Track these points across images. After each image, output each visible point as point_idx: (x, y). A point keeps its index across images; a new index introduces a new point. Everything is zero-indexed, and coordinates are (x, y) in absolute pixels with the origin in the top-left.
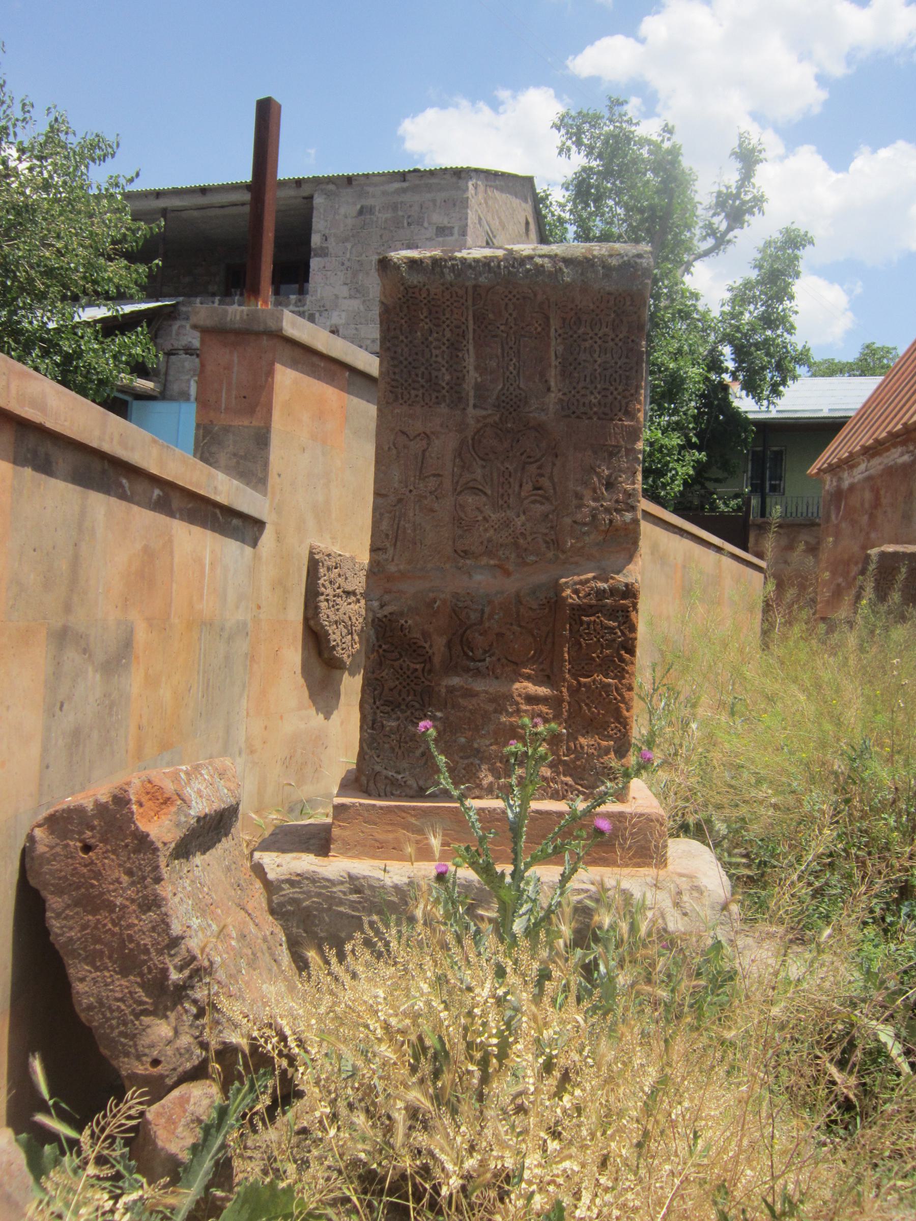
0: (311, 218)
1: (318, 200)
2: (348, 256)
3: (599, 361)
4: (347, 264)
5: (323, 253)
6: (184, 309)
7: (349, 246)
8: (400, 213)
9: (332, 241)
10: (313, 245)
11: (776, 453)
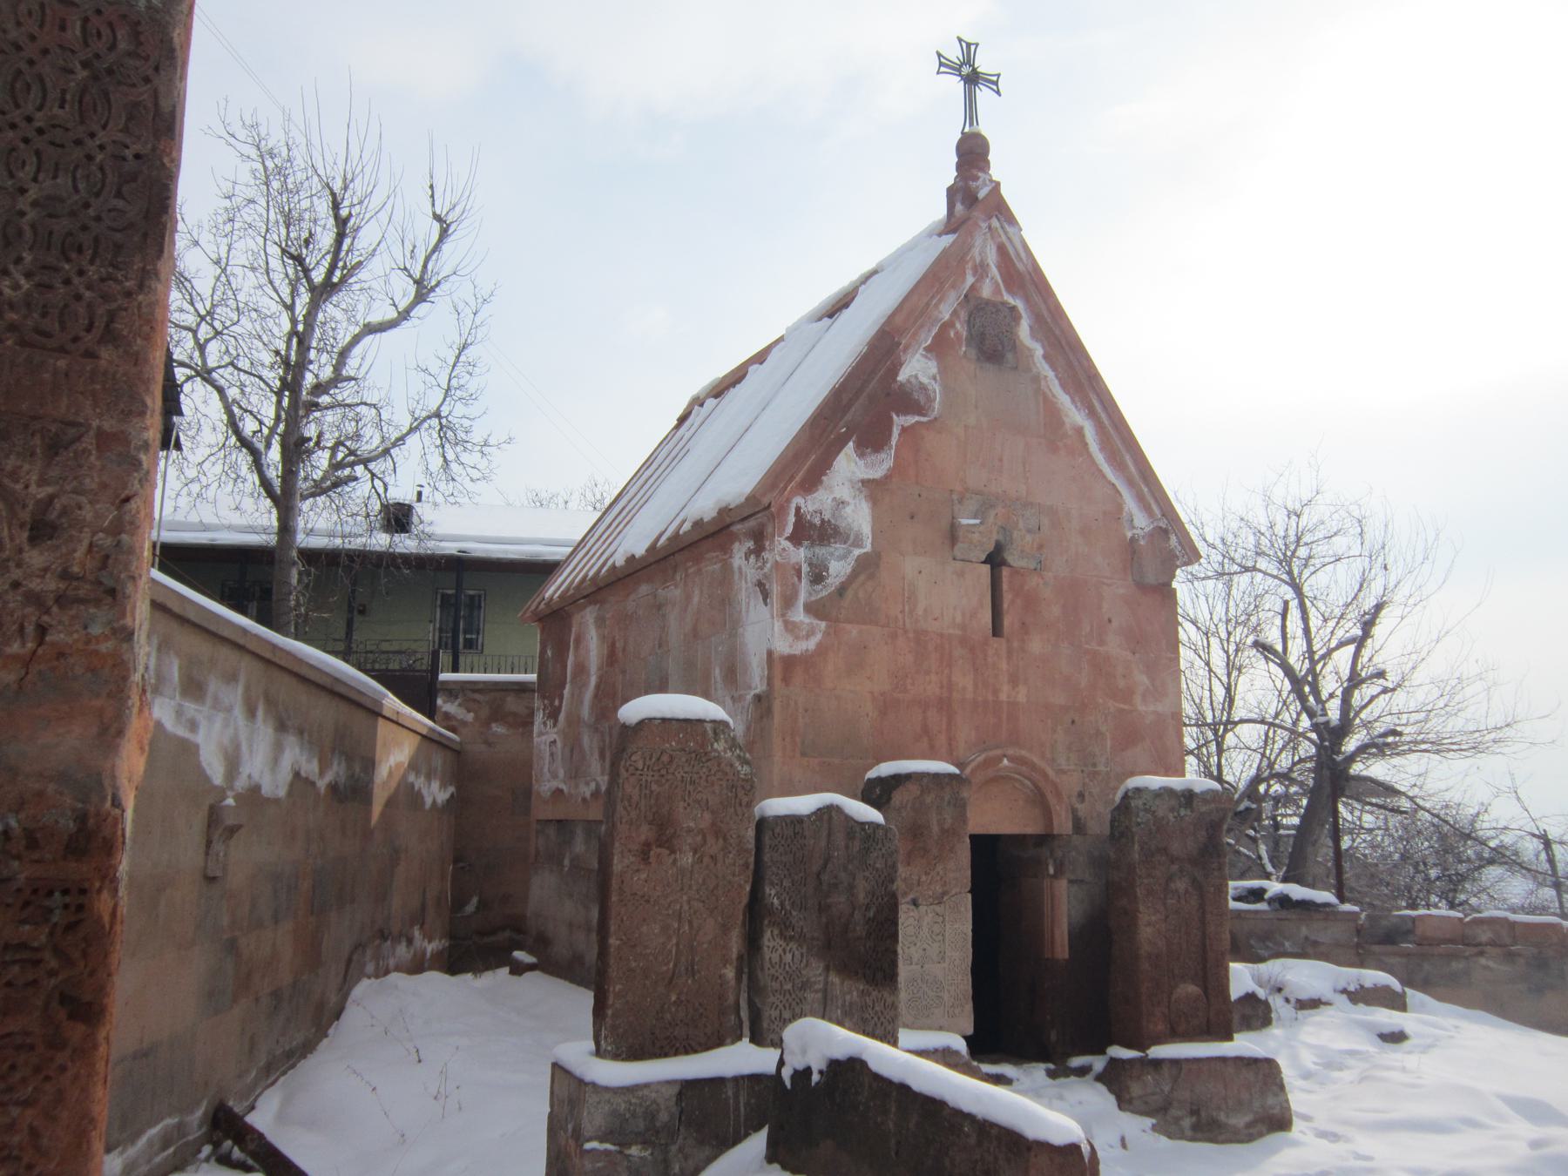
3: (33, 193)
11: (472, 597)
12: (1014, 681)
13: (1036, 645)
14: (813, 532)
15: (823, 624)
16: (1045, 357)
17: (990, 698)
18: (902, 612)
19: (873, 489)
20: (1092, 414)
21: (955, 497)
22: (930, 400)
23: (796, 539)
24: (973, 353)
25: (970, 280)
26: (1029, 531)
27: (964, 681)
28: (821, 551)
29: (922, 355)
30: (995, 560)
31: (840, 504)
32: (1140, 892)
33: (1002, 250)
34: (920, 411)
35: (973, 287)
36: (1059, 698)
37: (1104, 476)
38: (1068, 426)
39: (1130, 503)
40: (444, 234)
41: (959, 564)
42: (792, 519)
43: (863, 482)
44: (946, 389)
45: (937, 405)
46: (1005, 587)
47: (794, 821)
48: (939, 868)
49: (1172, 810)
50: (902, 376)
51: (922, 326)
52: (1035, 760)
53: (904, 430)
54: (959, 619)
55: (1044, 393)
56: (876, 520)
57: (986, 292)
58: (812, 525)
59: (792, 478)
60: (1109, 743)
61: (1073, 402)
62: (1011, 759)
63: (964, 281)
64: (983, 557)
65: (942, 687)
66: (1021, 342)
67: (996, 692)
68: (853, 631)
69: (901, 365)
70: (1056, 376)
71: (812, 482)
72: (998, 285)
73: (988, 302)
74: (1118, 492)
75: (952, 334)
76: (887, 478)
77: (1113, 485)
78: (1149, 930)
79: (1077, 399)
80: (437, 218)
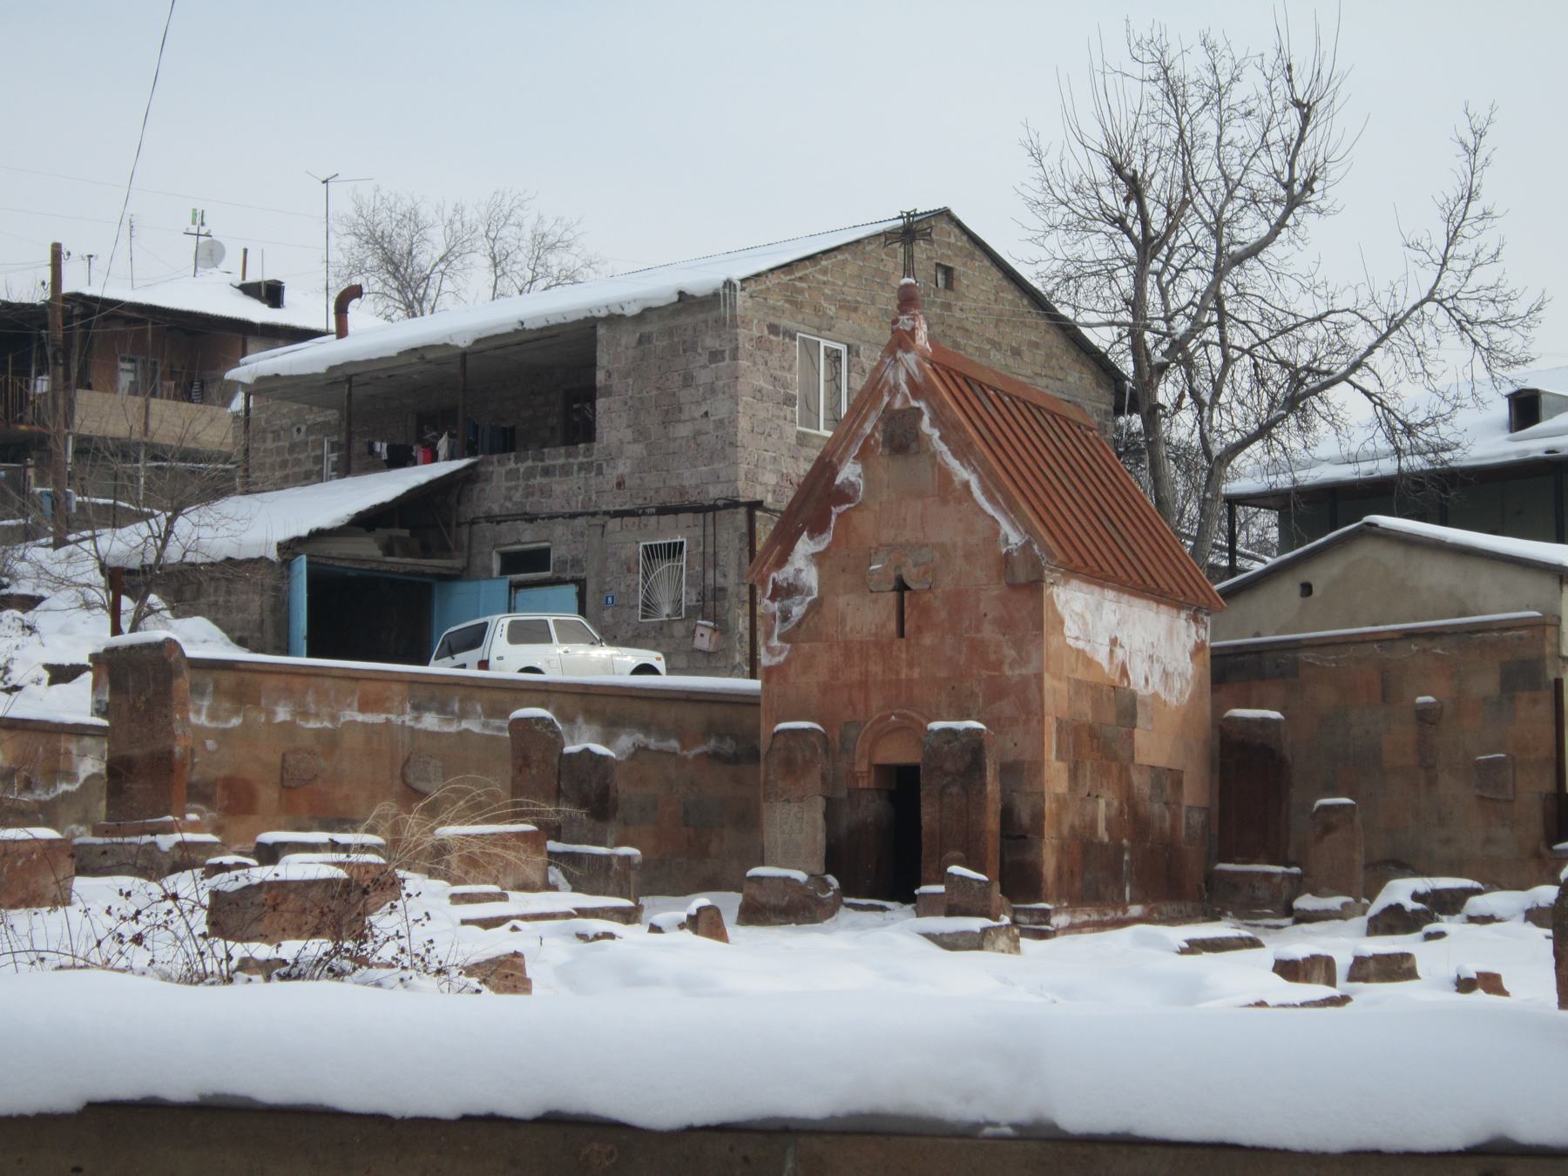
0: (595, 352)
1: (601, 331)
2: (630, 394)
4: (630, 403)
5: (608, 392)
6: (482, 469)
7: (630, 381)
8: (676, 339)
9: (615, 376)
10: (598, 385)
12: (911, 665)
13: (928, 640)
14: (785, 592)
15: (788, 646)
16: (941, 438)
17: (894, 677)
18: (837, 631)
19: (818, 559)
20: (975, 471)
21: (873, 551)
22: (856, 491)
23: (773, 598)
24: (887, 452)
25: (886, 399)
26: (916, 565)
27: (876, 668)
28: (786, 602)
29: (854, 463)
30: (902, 587)
31: (799, 571)
32: (922, 794)
33: (907, 372)
34: (849, 499)
35: (888, 404)
36: (942, 673)
37: (984, 512)
38: (957, 483)
39: (1006, 527)
40: (1306, 119)
41: (874, 595)
42: (770, 586)
43: (814, 555)
44: (867, 481)
45: (861, 494)
46: (906, 604)
47: (570, 755)
48: (802, 782)
49: (948, 742)
50: (838, 481)
51: (851, 442)
52: (914, 715)
53: (839, 516)
54: (873, 631)
55: (940, 466)
56: (820, 577)
57: (898, 404)
58: (782, 587)
59: (764, 564)
60: (981, 700)
61: (962, 464)
62: (897, 716)
63: (882, 400)
64: (891, 587)
65: (861, 674)
66: (923, 433)
67: (898, 673)
68: (806, 647)
69: (837, 473)
70: (949, 449)
71: (782, 561)
72: (906, 395)
73: (899, 411)
74: (997, 522)
75: (872, 442)
76: (828, 549)
78: (927, 817)
79: (964, 461)
80: (1297, 104)
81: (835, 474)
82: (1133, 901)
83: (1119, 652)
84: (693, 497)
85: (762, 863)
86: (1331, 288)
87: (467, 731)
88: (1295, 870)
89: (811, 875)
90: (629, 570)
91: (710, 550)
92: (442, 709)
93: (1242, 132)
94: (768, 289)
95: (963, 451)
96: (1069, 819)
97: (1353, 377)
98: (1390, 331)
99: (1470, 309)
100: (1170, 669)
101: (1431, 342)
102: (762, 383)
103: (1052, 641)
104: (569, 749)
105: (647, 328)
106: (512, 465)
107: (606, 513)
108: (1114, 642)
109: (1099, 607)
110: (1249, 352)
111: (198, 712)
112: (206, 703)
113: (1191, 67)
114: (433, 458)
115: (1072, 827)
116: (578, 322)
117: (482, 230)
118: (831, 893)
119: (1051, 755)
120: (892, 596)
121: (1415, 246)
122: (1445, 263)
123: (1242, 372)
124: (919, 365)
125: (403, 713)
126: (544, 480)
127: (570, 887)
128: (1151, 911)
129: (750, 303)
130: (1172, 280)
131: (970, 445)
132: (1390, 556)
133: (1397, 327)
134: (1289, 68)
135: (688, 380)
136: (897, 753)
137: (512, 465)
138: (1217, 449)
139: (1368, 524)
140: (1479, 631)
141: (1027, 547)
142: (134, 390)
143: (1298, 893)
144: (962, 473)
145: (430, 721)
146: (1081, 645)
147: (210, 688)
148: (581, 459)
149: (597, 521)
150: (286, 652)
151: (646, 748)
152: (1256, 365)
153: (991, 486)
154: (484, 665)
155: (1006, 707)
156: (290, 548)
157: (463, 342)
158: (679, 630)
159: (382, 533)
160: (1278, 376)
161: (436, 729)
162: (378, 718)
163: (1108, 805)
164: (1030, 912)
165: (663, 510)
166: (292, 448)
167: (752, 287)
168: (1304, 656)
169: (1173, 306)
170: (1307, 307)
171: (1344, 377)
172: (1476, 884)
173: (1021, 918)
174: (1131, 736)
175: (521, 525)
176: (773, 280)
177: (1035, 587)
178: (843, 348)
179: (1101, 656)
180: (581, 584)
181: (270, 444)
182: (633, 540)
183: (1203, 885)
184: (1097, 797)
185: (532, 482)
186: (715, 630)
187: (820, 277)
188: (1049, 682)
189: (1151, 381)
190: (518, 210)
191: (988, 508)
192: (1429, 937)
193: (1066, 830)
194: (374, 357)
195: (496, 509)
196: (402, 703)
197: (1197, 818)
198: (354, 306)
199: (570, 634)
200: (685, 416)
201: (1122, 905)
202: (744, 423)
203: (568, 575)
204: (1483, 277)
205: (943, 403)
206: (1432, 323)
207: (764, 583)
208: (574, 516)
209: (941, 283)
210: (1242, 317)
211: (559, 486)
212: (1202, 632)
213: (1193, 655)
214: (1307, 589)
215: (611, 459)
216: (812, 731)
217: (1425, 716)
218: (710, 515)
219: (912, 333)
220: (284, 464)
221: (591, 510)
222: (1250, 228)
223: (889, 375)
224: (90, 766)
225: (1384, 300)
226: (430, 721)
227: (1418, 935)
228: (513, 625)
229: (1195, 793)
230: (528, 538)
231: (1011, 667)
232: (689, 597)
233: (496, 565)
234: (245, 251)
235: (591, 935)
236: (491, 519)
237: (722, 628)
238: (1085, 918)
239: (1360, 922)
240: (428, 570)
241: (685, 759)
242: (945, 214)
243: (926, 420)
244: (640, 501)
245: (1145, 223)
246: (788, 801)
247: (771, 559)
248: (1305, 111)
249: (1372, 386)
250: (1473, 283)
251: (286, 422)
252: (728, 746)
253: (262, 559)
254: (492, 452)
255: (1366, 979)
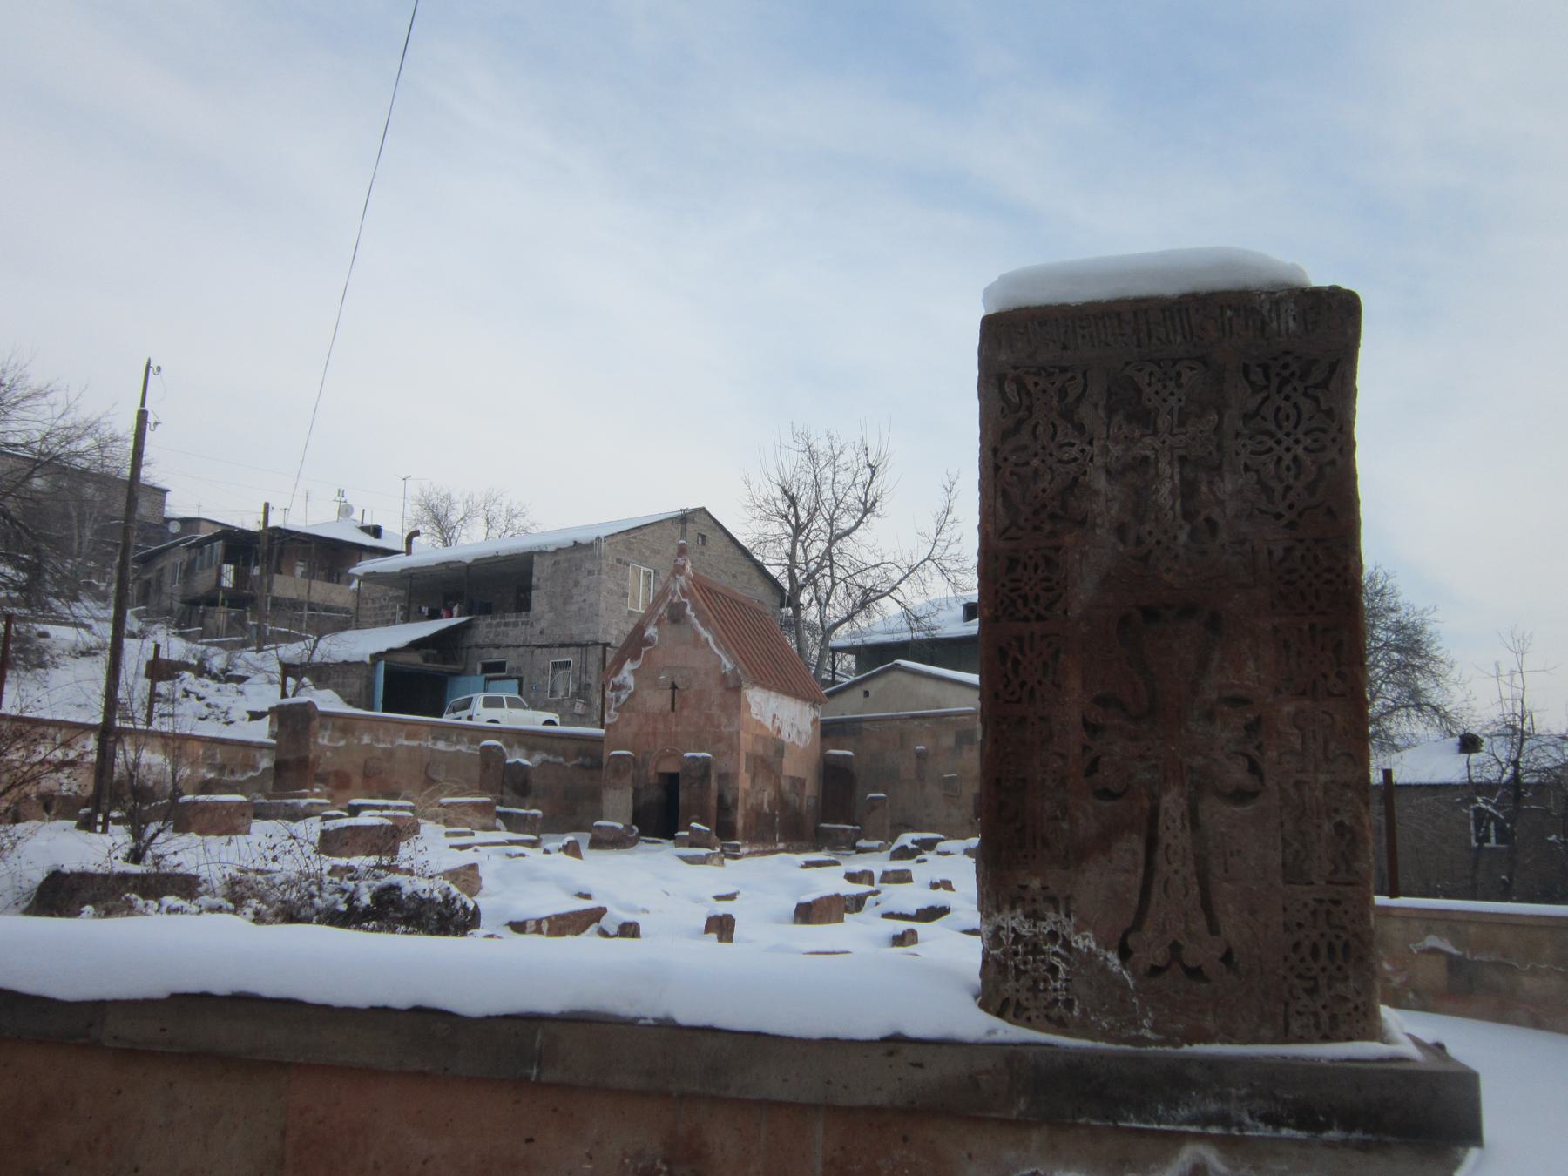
5: (538, 588)
7: (549, 583)
9: (541, 580)
12: (677, 725)
13: (685, 713)
14: (618, 688)
15: (618, 714)
16: (695, 617)
19: (635, 672)
22: (654, 641)
23: (612, 691)
27: (660, 726)
28: (619, 693)
30: (674, 687)
31: (625, 678)
34: (650, 644)
35: (671, 600)
37: (714, 653)
39: (724, 660)
40: (873, 473)
43: (633, 671)
47: (509, 764)
50: (646, 635)
51: (652, 617)
52: (679, 750)
53: (646, 652)
57: (676, 600)
68: (627, 715)
71: (616, 673)
74: (720, 658)
76: (639, 668)
77: (718, 656)
80: (870, 466)
81: (644, 632)
82: (780, 841)
83: (776, 721)
84: (576, 639)
85: (601, 818)
86: (883, 551)
87: (459, 751)
88: (858, 827)
89: (625, 826)
90: (544, 674)
91: (584, 665)
92: (447, 739)
93: (844, 478)
94: (617, 542)
95: (705, 624)
96: (751, 801)
97: (892, 594)
98: (910, 573)
99: (947, 564)
100: (801, 730)
101: (928, 579)
102: (612, 586)
103: (745, 715)
104: (510, 761)
105: (558, 558)
106: (489, 621)
107: (534, 646)
108: (774, 716)
109: (768, 699)
110: (844, 580)
111: (323, 737)
112: (328, 733)
113: (821, 446)
114: (451, 616)
115: (752, 805)
116: (525, 553)
117: (482, 506)
118: (634, 835)
119: (742, 770)
120: (669, 692)
121: (923, 534)
122: (936, 542)
123: (840, 589)
124: (686, 582)
125: (428, 741)
126: (505, 629)
127: (505, 829)
128: (789, 846)
129: (608, 548)
130: (809, 545)
131: (709, 621)
132: (906, 679)
133: (913, 571)
134: (866, 449)
135: (576, 584)
136: (669, 767)
137: (489, 621)
138: (827, 626)
139: (896, 664)
140: (947, 716)
141: (734, 671)
142: (304, 575)
143: (859, 839)
144: (705, 634)
145: (441, 745)
146: (758, 718)
147: (330, 726)
148: (523, 619)
149: (531, 649)
150: (371, 708)
151: (547, 761)
152: (847, 586)
153: (718, 641)
154: (470, 718)
155: (722, 747)
156: (376, 657)
157: (468, 560)
158: (567, 704)
159: (424, 651)
160: (858, 592)
161: (444, 749)
162: (415, 743)
163: (769, 794)
164: (730, 846)
165: (562, 645)
166: (381, 608)
167: (609, 540)
168: (866, 726)
169: (809, 558)
170: (872, 561)
171: (888, 594)
172: (942, 836)
173: (726, 849)
174: (781, 762)
175: (491, 649)
176: (619, 538)
177: (737, 689)
178: (652, 571)
179: (768, 723)
180: (520, 680)
181: (369, 606)
182: (546, 659)
183: (814, 834)
184: (764, 791)
185: (498, 629)
186: (584, 704)
187: (642, 537)
188: (742, 734)
189: (796, 593)
190: (501, 498)
191: (716, 650)
192: (919, 861)
193: (749, 806)
194: (424, 565)
195: (480, 642)
196: (428, 736)
197: (812, 802)
198: (416, 539)
199: (513, 704)
200: (574, 601)
201: (774, 842)
202: (603, 605)
203: (514, 675)
204: (953, 550)
205: (697, 601)
206: (929, 570)
207: (608, 682)
208: (519, 646)
209: (700, 542)
210: (841, 564)
211: (512, 632)
212: (817, 713)
213: (812, 724)
214: (867, 694)
215: (538, 620)
216: (628, 756)
217: (921, 756)
218: (584, 649)
219: (684, 567)
220: (376, 615)
221: (527, 644)
222: (846, 522)
223: (672, 586)
224: (265, 763)
225: (907, 559)
226: (441, 745)
227: (914, 860)
228: (485, 698)
229: (811, 790)
230: (495, 656)
231: (725, 728)
232: (572, 688)
233: (479, 668)
234: (364, 510)
235: (513, 854)
236: (477, 646)
237: (588, 703)
238: (756, 849)
239: (887, 853)
240: (445, 671)
241: (566, 767)
242: (703, 510)
243: (689, 608)
244: (551, 641)
245: (797, 518)
246: (615, 789)
247: (612, 672)
248: (873, 469)
249: (901, 598)
250: (948, 552)
251: (378, 595)
252: (588, 761)
253: (362, 663)
254: (480, 614)
255: (888, 882)
